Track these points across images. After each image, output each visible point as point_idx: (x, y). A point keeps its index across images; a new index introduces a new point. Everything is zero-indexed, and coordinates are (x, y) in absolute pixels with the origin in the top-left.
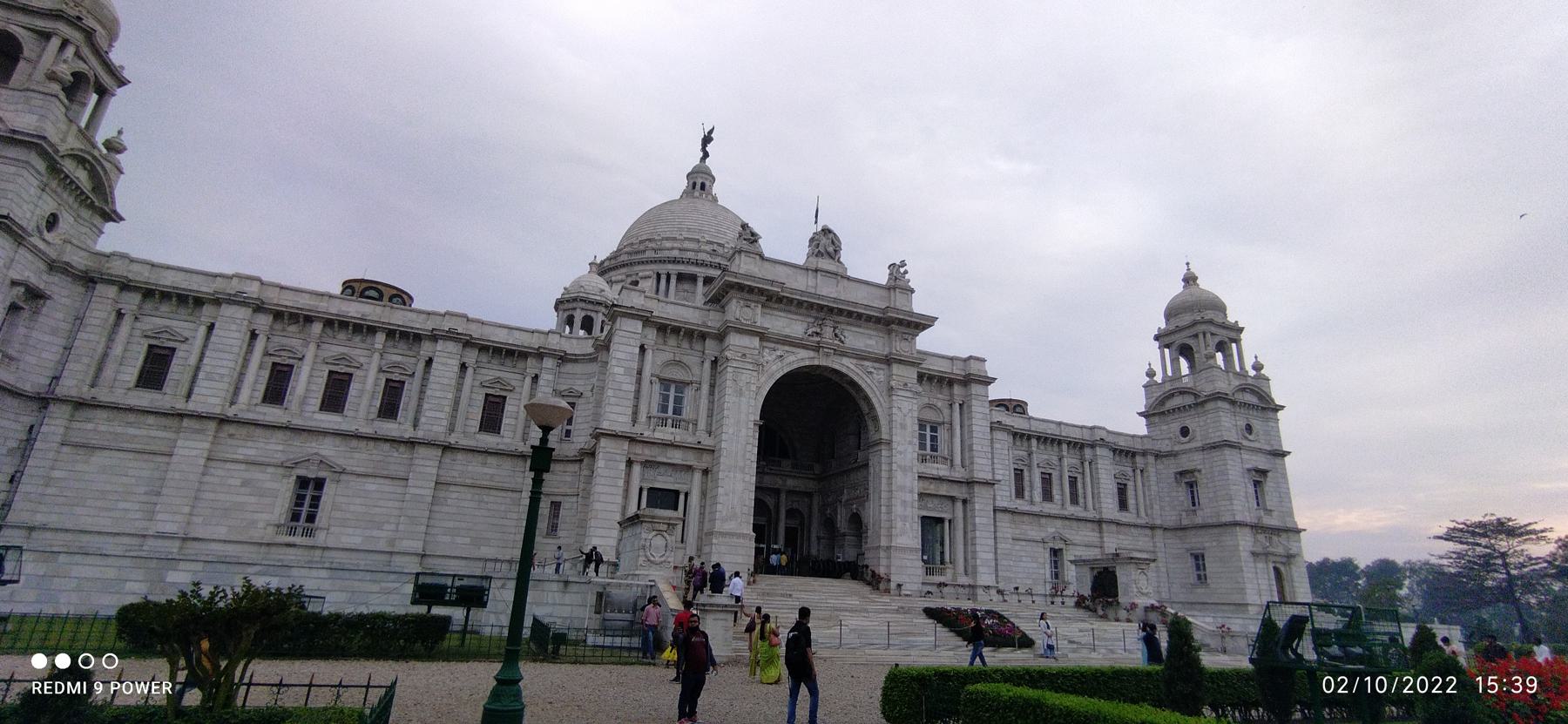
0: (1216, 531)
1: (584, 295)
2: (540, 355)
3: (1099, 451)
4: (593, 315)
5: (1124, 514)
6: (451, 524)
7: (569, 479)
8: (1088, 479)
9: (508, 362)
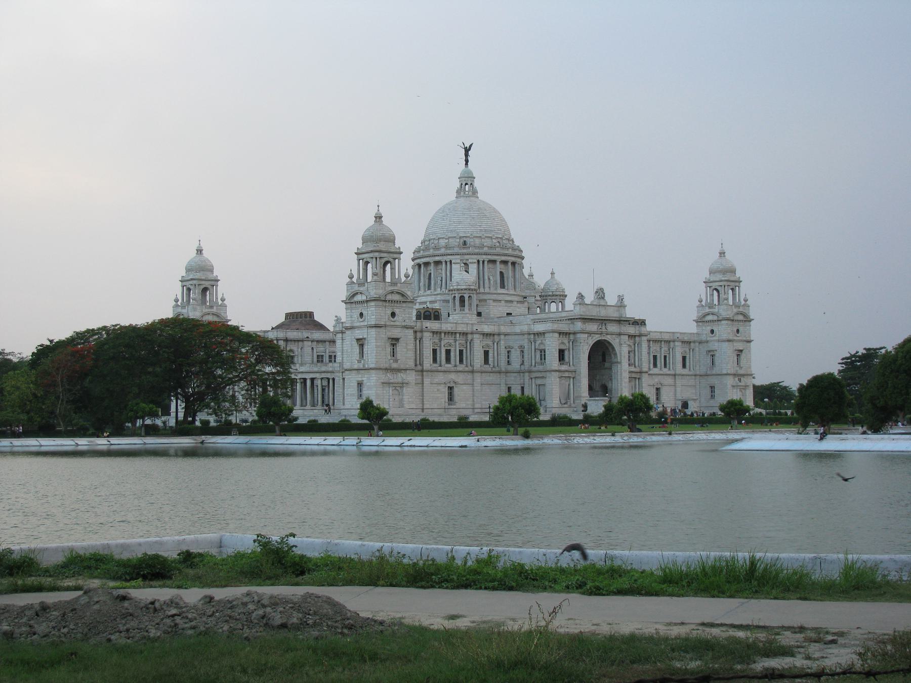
0: (719, 377)
1: (468, 287)
2: (499, 334)
3: (677, 343)
4: (472, 295)
5: (684, 370)
6: (484, 398)
7: (513, 378)
8: (671, 356)
9: (488, 337)
